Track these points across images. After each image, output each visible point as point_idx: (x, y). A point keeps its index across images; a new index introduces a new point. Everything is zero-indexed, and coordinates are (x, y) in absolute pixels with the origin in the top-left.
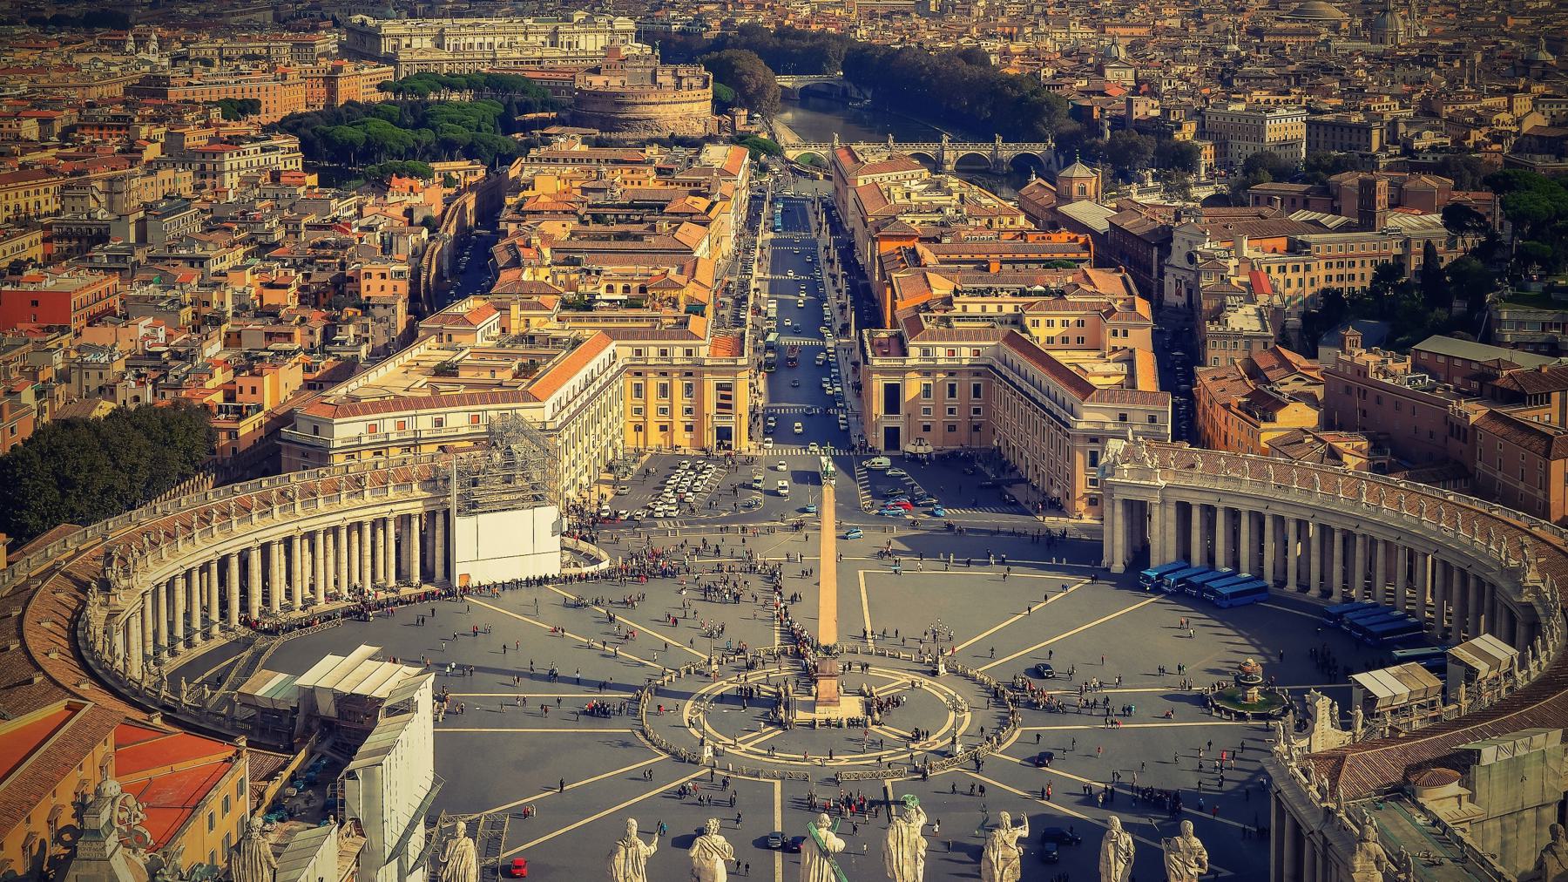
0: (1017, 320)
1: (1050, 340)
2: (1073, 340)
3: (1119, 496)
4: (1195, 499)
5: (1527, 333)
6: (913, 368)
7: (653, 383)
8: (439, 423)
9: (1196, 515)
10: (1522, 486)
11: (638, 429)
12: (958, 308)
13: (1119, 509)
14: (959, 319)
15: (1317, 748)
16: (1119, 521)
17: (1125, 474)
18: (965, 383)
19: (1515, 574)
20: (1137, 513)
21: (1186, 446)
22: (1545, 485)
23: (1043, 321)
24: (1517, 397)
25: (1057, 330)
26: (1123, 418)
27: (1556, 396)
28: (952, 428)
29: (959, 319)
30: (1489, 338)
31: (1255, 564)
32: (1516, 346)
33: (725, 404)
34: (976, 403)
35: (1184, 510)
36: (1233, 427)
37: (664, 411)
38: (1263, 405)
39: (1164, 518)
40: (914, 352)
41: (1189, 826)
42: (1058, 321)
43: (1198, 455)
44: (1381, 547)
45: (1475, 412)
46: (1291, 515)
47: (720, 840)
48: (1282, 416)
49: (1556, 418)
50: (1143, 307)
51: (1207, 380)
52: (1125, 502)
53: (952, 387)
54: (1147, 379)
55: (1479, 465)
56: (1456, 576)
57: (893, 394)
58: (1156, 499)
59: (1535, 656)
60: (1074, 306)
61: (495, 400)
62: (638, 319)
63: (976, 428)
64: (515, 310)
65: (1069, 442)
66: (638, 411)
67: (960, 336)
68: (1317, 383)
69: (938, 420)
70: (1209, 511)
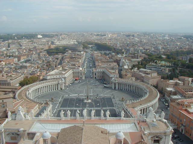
5: (149, 68)
9: (120, 84)
17: (114, 81)
20: (115, 84)
22: (149, 81)
24: (147, 74)
30: (146, 69)
35: (119, 84)
36: (124, 77)
45: (143, 75)
57: (95, 74)
61: (60, 74)
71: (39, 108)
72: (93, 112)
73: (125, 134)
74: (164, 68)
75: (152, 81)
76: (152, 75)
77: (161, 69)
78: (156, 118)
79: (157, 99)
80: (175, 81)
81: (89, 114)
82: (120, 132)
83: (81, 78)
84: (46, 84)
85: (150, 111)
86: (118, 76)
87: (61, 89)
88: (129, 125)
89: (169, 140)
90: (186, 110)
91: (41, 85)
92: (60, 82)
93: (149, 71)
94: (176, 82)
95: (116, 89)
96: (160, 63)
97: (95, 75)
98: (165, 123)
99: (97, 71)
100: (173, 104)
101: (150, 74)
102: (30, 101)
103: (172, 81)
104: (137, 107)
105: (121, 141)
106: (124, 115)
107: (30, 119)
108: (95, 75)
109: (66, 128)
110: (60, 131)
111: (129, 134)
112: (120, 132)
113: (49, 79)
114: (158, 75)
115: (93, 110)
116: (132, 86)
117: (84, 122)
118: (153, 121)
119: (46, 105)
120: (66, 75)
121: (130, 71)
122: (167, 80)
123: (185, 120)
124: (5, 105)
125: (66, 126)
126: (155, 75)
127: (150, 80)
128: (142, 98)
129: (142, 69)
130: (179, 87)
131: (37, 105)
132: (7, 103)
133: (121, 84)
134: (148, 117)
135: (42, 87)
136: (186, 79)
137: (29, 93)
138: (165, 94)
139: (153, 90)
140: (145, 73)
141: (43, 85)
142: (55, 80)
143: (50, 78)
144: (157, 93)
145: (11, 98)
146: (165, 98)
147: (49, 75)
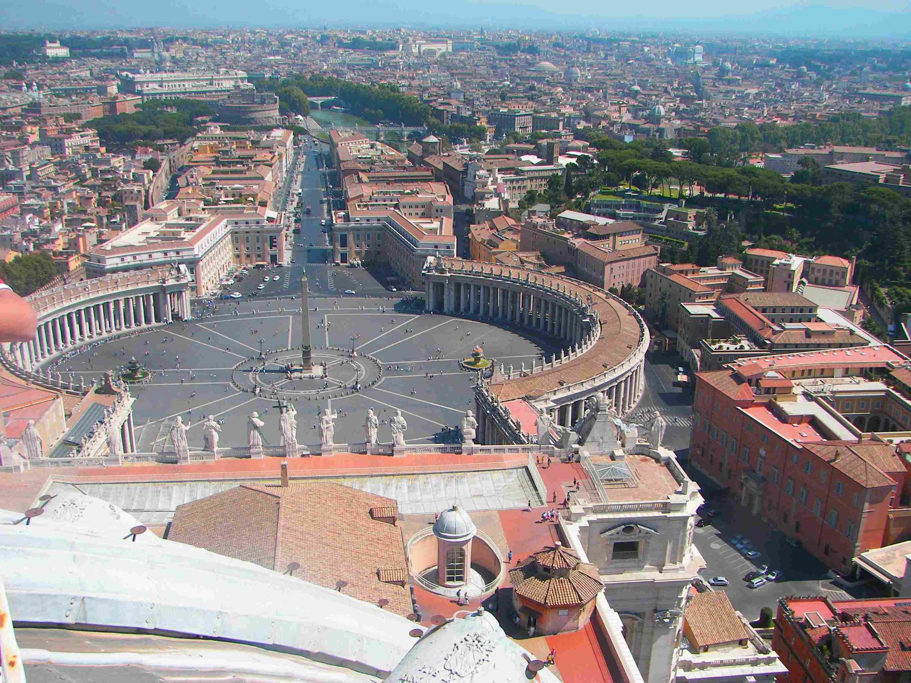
5: (604, 210)
6: (353, 229)
8: (150, 256)
9: (462, 288)
10: (594, 274)
11: (238, 256)
13: (431, 286)
15: (493, 382)
16: (431, 291)
17: (434, 273)
19: (583, 311)
21: (460, 259)
22: (603, 273)
27: (611, 238)
30: (588, 211)
32: (598, 215)
35: (458, 286)
36: (483, 251)
39: (449, 289)
41: (400, 413)
45: (578, 243)
47: (214, 424)
49: (611, 245)
50: (450, 199)
51: (472, 230)
59: (586, 343)
61: (173, 246)
62: (237, 208)
63: (379, 253)
64: (186, 207)
68: (519, 231)
70: (468, 287)
71: (68, 416)
73: (481, 518)
74: (675, 207)
76: (618, 243)
77: (661, 211)
78: (623, 445)
79: (638, 358)
80: (728, 272)
82: (454, 509)
83: (274, 259)
84: (101, 294)
85: (598, 410)
87: (176, 317)
88: (497, 475)
89: (683, 542)
90: (772, 408)
91: (74, 302)
92: (171, 282)
93: (602, 221)
94: (733, 278)
95: (445, 310)
96: (655, 186)
97: (344, 244)
98: (668, 463)
99: (352, 224)
100: (708, 377)
101: (606, 237)
102: (23, 382)
103: (711, 271)
104: (546, 396)
105: (462, 554)
106: (474, 432)
107: (25, 465)
109: (202, 501)
110: (171, 515)
111: (497, 519)
112: (454, 509)
113: (114, 271)
114: (646, 244)
117: (284, 467)
118: (613, 457)
119: (102, 399)
120: (198, 250)
121: (511, 222)
122: (688, 266)
123: (762, 452)
125: (204, 491)
126: (635, 242)
127: (607, 268)
128: (566, 354)
129: (568, 214)
130: (742, 297)
131: (61, 399)
133: (468, 287)
135: (79, 312)
136: (777, 262)
138: (676, 331)
139: (623, 312)
140: (583, 230)
141: (82, 299)
142: (144, 271)
143: (120, 265)
144: (642, 331)
146: (678, 350)
147: (115, 250)
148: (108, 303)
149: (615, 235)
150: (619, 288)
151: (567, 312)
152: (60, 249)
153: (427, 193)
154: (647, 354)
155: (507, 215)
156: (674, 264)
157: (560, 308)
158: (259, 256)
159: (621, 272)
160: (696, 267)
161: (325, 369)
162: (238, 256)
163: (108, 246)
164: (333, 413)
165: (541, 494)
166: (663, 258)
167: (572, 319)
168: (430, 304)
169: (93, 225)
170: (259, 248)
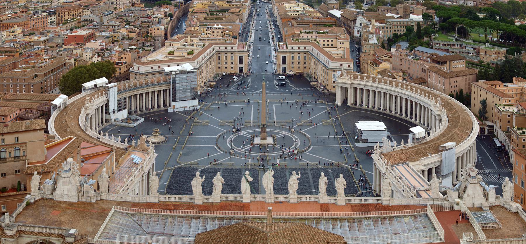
0: (315, 40)
1: (324, 45)
2: (330, 46)
3: (340, 85)
4: (358, 87)
6: (290, 52)
7: (223, 56)
9: (358, 90)
12: (301, 36)
13: (340, 89)
14: (301, 39)
18: (302, 56)
20: (344, 90)
23: (322, 40)
25: (326, 43)
26: (341, 65)
27: (448, 62)
28: (299, 68)
29: (301, 39)
31: (373, 103)
33: (241, 61)
34: (305, 61)
35: (355, 89)
36: (370, 69)
37: (226, 63)
38: (376, 63)
40: (290, 47)
42: (326, 40)
43: (359, 75)
44: (404, 100)
46: (382, 91)
48: (380, 66)
50: (347, 36)
51: (363, 56)
52: (341, 87)
53: (299, 57)
54: (348, 55)
55: (429, 79)
56: (422, 107)
58: (349, 86)
60: (330, 36)
62: (220, 39)
63: (305, 67)
65: (328, 72)
66: (220, 63)
67: (301, 44)
69: (295, 65)
70: (362, 90)
72: (293, 182)
75: (453, 84)
79: (472, 140)
81: (281, 187)
83: (241, 70)
86: (352, 66)
97: (284, 61)
103: (510, 85)
108: (284, 61)
113: (147, 74)
115: (294, 173)
116: (396, 98)
117: (270, 211)
121: (385, 51)
124: (21, 151)
132: (29, 148)
134: (465, 195)
137: (87, 115)
145: (40, 129)
148: (142, 94)
149: (450, 61)
150: (455, 94)
151: (425, 108)
152: (117, 60)
153: (334, 33)
154: (479, 137)
155: (383, 47)
156: (487, 80)
157: (420, 105)
158: (232, 68)
159: (457, 84)
160: (500, 82)
161: (274, 140)
162: (219, 68)
163: (144, 59)
164: (297, 174)
165: (440, 234)
166: (480, 76)
167: (428, 112)
168: (339, 101)
169: (135, 47)
170: (232, 63)
